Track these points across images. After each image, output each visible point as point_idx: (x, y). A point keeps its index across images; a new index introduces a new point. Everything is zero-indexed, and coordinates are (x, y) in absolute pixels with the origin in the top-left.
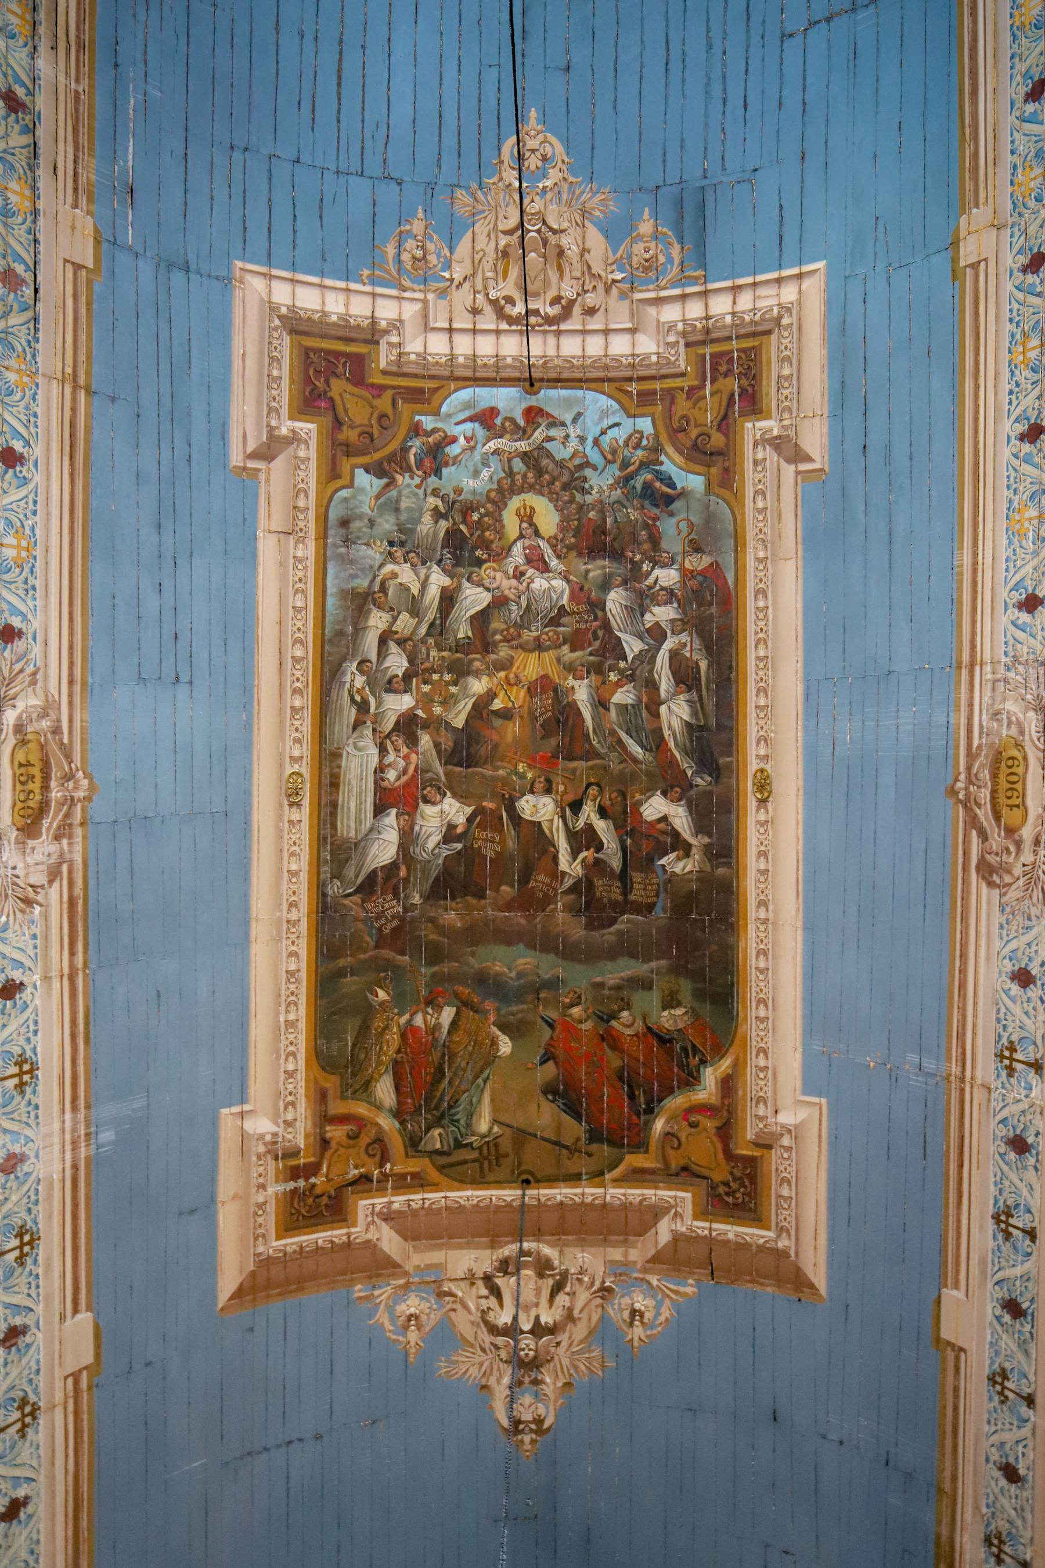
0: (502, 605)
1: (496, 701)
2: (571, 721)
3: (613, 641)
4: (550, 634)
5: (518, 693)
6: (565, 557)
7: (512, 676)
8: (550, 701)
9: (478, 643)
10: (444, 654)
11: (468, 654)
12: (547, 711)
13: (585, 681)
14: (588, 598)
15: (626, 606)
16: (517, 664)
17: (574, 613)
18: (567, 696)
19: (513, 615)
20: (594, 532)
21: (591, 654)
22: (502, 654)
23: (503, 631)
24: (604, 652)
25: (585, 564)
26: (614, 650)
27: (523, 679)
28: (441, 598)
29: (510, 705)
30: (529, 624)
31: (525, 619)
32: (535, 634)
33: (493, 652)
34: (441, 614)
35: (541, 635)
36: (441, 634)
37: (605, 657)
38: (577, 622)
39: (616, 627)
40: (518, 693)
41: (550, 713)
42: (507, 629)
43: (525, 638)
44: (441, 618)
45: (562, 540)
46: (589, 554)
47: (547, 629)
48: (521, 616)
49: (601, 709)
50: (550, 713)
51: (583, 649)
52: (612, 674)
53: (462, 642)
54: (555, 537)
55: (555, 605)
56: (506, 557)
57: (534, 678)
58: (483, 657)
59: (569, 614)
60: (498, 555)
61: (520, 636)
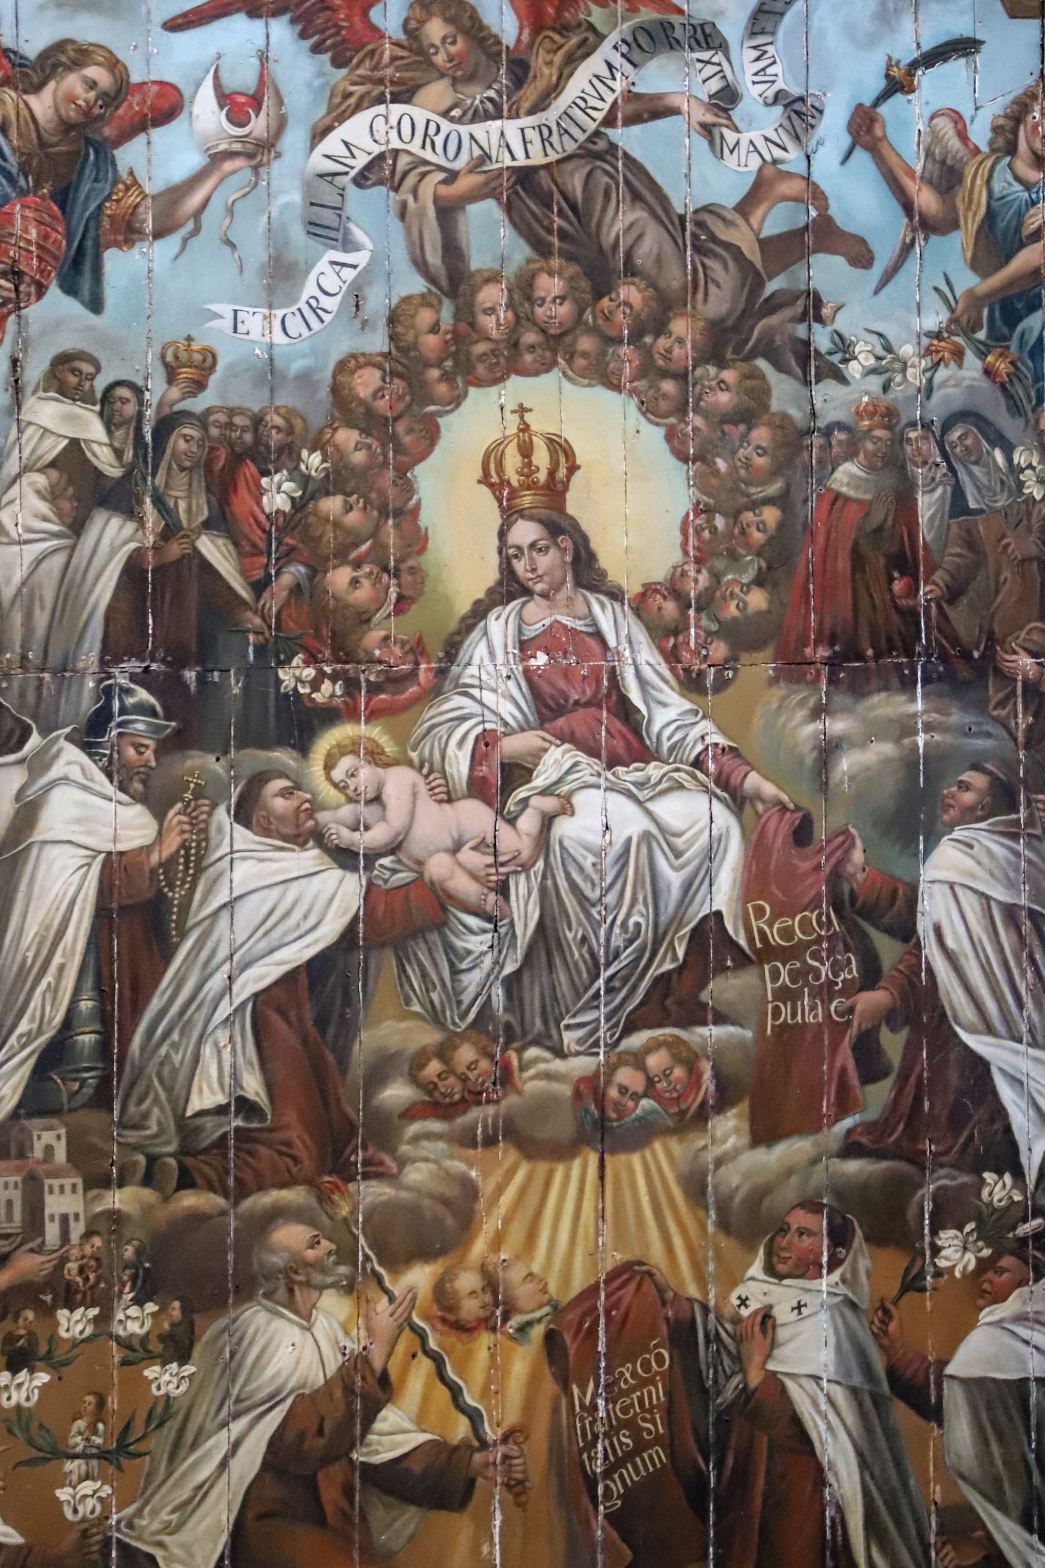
0: (418, 932)
1: (389, 1418)
2: (760, 1483)
3: (954, 1077)
4: (655, 1061)
5: (497, 1368)
6: (721, 685)
7: (467, 1281)
8: (657, 1393)
9: (296, 1133)
10: (119, 1199)
11: (242, 1191)
12: (641, 1446)
13: (825, 1283)
14: (836, 877)
15: (1010, 912)
16: (489, 1226)
17: (767, 953)
18: (738, 1359)
19: (472, 980)
20: (858, 559)
21: (850, 1149)
22: (416, 1175)
23: (420, 1059)
24: (912, 1133)
25: (818, 712)
26: (957, 1119)
27: (524, 1293)
28: (102, 914)
29: (461, 1429)
30: (552, 1014)
31: (533, 996)
32: (581, 1065)
33: (374, 1172)
34: (103, 995)
35: (611, 1069)
36: (102, 1099)
37: (916, 1159)
38: (784, 994)
39: (967, 1012)
40: (497, 1368)
41: (658, 1455)
42: (444, 1052)
43: (531, 1086)
44: (104, 1016)
45: (706, 603)
46: (832, 663)
47: (638, 1040)
48: (512, 983)
49: (902, 1414)
50: (658, 1455)
51: (812, 1124)
52: (948, 1237)
53: (212, 1130)
54: (674, 589)
55: (678, 919)
56: (435, 692)
57: (578, 1284)
58: (324, 1197)
59: (743, 960)
60: (394, 681)
61: (505, 1078)
